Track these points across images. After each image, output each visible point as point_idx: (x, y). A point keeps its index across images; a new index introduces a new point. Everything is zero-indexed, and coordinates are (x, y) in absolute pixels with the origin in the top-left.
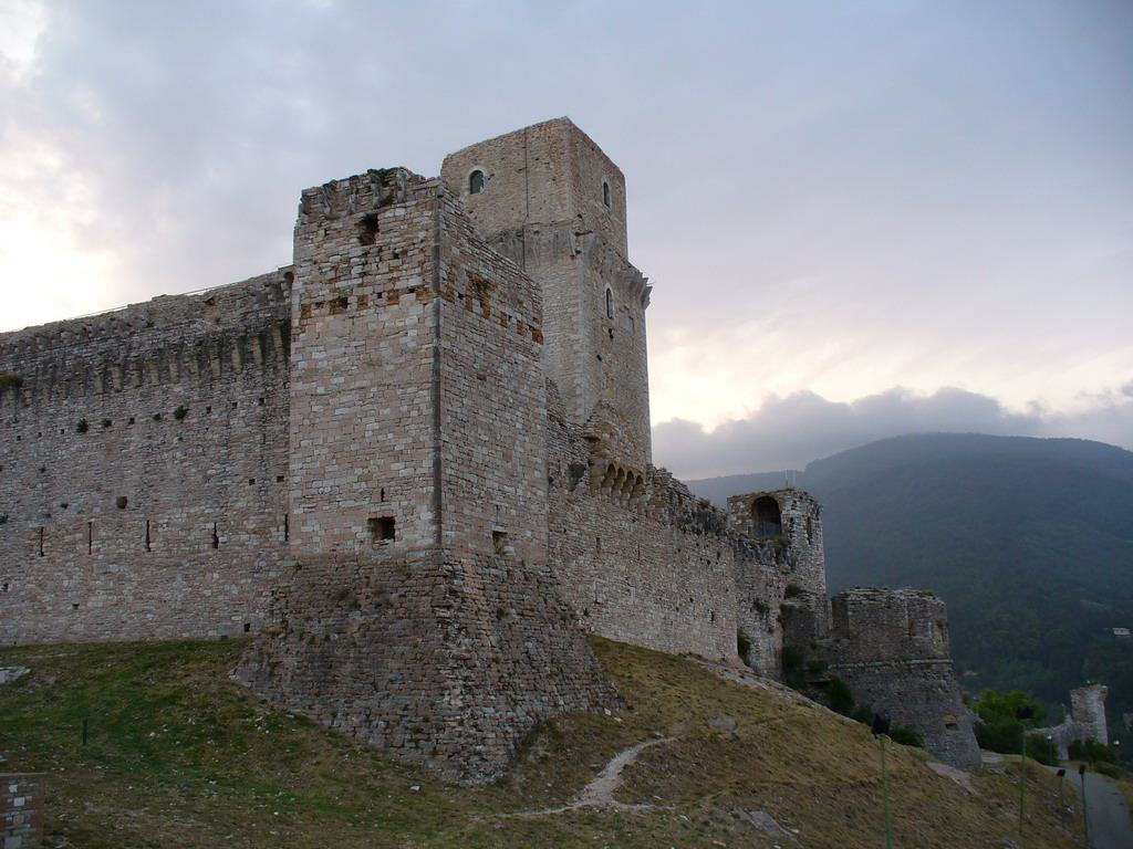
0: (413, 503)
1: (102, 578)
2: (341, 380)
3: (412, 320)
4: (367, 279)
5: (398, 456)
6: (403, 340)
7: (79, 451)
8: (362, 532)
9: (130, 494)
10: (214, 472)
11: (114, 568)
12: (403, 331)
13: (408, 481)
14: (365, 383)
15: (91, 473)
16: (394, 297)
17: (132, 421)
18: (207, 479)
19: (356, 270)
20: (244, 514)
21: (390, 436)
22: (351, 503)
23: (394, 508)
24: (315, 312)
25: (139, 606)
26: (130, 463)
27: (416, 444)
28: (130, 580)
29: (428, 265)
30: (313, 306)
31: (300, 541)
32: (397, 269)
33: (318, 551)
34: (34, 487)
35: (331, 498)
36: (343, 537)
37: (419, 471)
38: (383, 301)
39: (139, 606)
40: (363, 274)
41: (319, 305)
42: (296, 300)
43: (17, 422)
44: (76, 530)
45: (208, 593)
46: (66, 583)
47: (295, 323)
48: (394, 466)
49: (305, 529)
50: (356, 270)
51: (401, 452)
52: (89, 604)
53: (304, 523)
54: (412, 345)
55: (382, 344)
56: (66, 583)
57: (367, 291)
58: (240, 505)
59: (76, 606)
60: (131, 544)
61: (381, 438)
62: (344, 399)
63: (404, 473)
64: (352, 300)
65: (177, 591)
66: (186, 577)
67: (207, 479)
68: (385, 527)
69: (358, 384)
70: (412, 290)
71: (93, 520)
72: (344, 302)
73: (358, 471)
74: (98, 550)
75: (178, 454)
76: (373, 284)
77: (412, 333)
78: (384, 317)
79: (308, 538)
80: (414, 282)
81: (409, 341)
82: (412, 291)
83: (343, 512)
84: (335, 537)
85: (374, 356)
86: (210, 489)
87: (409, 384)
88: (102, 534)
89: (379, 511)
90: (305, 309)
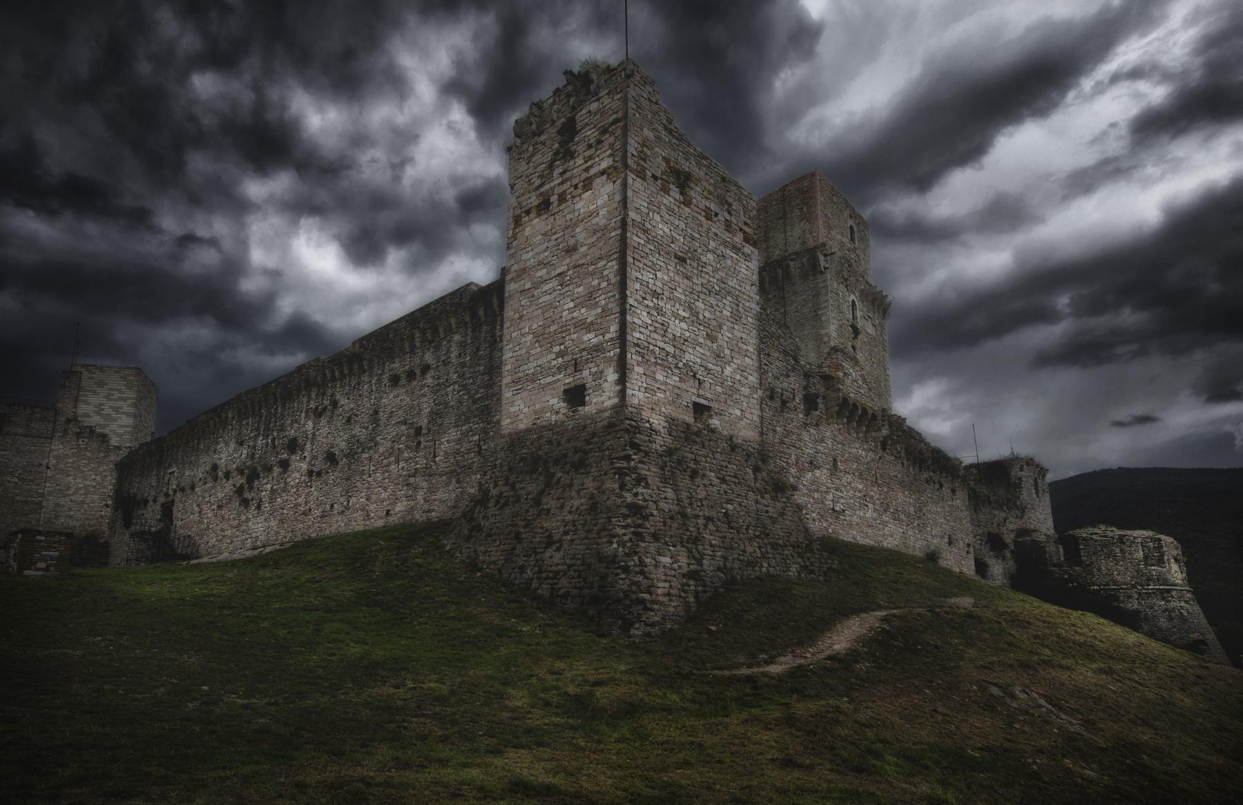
0: (601, 367)
6: (594, 221)
8: (556, 402)
9: (424, 422)
10: (480, 395)
11: (412, 480)
13: (598, 349)
15: (401, 412)
18: (475, 402)
21: (583, 310)
22: (549, 379)
29: (618, 145)
30: (523, 215)
31: (509, 421)
32: (590, 158)
36: (543, 410)
37: (608, 336)
48: (586, 338)
49: (512, 410)
51: (592, 323)
55: (578, 230)
61: (575, 314)
62: (546, 288)
63: (595, 341)
64: (554, 199)
66: (458, 481)
67: (475, 402)
68: (576, 396)
69: (558, 271)
73: (556, 349)
77: (603, 212)
83: (543, 387)
84: (536, 412)
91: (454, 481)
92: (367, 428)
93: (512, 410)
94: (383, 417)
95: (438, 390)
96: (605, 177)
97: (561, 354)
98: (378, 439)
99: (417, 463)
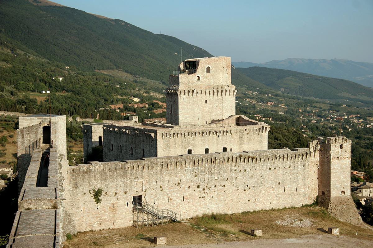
1: (276, 197)
2: (338, 170)
4: (342, 155)
5: (346, 182)
6: (346, 165)
11: (278, 196)
14: (341, 171)
18: (294, 179)
19: (340, 153)
20: (301, 186)
22: (339, 189)
23: (345, 190)
24: (334, 159)
25: (283, 202)
26: (280, 176)
28: (281, 198)
33: (335, 196)
35: (336, 188)
36: (338, 194)
38: (344, 158)
39: (283, 202)
40: (341, 154)
41: (335, 158)
42: (331, 157)
43: (254, 166)
44: (270, 189)
45: (296, 199)
46: (268, 199)
47: (331, 160)
48: (345, 184)
49: (333, 193)
50: (340, 153)
52: (274, 202)
53: (333, 192)
56: (268, 199)
57: (342, 157)
58: (301, 184)
65: (290, 200)
66: (292, 197)
67: (294, 179)
71: (273, 187)
72: (338, 158)
76: (343, 156)
79: (333, 194)
80: (348, 156)
83: (338, 190)
85: (342, 167)
86: (295, 181)
88: (275, 189)
89: (343, 190)
91: (291, 197)
93: (333, 193)
95: (283, 174)
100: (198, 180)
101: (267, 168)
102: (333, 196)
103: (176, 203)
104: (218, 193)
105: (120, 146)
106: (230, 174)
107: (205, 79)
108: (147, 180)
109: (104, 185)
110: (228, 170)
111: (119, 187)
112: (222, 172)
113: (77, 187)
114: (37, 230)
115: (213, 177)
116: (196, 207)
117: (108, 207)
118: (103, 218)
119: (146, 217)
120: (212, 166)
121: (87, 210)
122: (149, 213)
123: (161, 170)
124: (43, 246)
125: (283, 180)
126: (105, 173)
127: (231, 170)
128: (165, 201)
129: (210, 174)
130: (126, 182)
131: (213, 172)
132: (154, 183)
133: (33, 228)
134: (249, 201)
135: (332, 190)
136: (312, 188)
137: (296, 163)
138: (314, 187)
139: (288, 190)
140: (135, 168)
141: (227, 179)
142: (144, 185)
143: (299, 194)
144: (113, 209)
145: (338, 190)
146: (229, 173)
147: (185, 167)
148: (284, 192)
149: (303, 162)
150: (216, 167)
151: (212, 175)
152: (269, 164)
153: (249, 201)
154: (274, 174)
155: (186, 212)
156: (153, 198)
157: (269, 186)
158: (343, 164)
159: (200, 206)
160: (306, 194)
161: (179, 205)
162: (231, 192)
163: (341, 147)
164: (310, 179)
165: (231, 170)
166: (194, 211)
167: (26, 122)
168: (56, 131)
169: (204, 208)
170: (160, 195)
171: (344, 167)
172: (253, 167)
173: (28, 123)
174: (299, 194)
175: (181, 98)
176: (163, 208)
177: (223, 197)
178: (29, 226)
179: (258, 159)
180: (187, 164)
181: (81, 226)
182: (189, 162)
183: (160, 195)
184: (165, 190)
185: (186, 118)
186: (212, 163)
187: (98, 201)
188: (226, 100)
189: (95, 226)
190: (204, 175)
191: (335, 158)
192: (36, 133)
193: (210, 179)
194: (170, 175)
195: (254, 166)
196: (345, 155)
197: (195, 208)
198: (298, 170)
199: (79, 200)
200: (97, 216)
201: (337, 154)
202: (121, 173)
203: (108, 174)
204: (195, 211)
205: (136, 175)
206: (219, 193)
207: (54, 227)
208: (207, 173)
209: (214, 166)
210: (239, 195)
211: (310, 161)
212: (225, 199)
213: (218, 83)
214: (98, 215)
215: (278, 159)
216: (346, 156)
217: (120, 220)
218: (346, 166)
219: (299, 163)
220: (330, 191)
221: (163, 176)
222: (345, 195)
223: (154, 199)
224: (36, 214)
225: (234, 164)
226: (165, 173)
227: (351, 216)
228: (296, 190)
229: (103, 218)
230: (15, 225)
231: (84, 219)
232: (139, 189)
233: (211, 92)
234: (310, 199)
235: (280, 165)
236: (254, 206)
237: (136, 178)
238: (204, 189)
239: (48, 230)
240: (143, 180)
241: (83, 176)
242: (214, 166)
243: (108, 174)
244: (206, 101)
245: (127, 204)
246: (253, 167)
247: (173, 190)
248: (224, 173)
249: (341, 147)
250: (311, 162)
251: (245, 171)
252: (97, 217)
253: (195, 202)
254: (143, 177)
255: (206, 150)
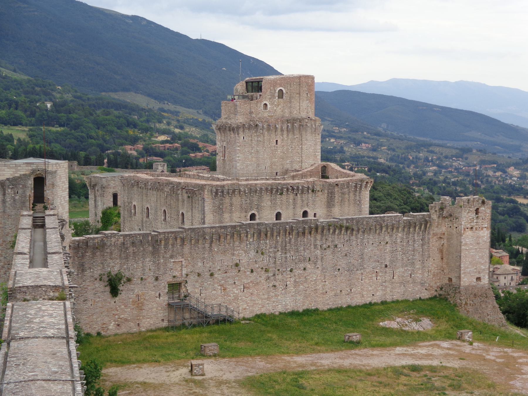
2: (472, 246)
3: (485, 234)
4: (478, 224)
5: (482, 264)
7: (371, 250)
8: (475, 280)
9: (388, 264)
12: (484, 237)
13: (484, 270)
16: (482, 229)
17: (387, 243)
19: (475, 221)
22: (473, 274)
23: (481, 275)
24: (467, 230)
26: (387, 255)
27: (486, 262)
33: (466, 285)
34: (358, 261)
35: (469, 273)
38: (480, 229)
39: (391, 294)
41: (467, 228)
43: (350, 240)
44: (373, 273)
45: (410, 290)
46: (370, 288)
47: (462, 232)
49: (464, 280)
50: (475, 221)
52: (377, 294)
54: (485, 240)
56: (370, 288)
57: (477, 226)
58: (417, 267)
59: (373, 295)
60: (388, 277)
64: (474, 228)
66: (404, 286)
68: (478, 279)
70: (485, 227)
73: (475, 267)
74: (379, 279)
75: (401, 253)
77: (486, 237)
78: (480, 233)
80: (486, 226)
81: (485, 239)
82: (485, 227)
83: (472, 276)
84: (470, 281)
85: (478, 242)
86: (409, 262)
87: (485, 249)
89: (478, 276)
90: (464, 229)
91: (402, 286)
92: (358, 261)
93: (464, 280)
94: (366, 258)
95: (392, 252)
96: (486, 229)
97: (476, 269)
98: (365, 266)
99: (385, 278)
100: (265, 261)
101: (368, 242)
102: (464, 284)
103: (232, 295)
104: (295, 281)
105: (148, 208)
106: (314, 252)
107: (275, 108)
108: (189, 259)
109: (125, 267)
110: (311, 245)
111: (147, 270)
112: (302, 248)
113: (83, 271)
114: (41, 331)
115: (288, 256)
116: (262, 299)
117: (131, 300)
118: (122, 316)
119: (187, 316)
120: (287, 240)
121: (100, 304)
122: (192, 309)
123: (211, 246)
124: (54, 354)
125: (392, 262)
126: (127, 248)
127: (315, 246)
128: (214, 292)
129: (284, 251)
130: (158, 262)
131: (288, 248)
132: (200, 264)
133: (35, 328)
134: (341, 291)
135: (462, 276)
136: (434, 273)
137: (411, 235)
138: (436, 271)
139: (398, 276)
140: (171, 242)
141: (309, 260)
142: (185, 267)
143: (414, 282)
144: (139, 304)
145: (472, 276)
146: (313, 249)
147: (247, 241)
148: (393, 278)
149: (421, 234)
150: (293, 240)
151: (286, 253)
152: (371, 238)
153: (341, 291)
154: (378, 253)
155: (247, 307)
156: (198, 287)
157: (371, 269)
158: (480, 238)
159: (268, 299)
160: (425, 282)
161: (236, 298)
162: (314, 278)
163: (477, 211)
164: (431, 259)
165: (315, 246)
166: (259, 306)
167: (8, 170)
168: (53, 185)
169: (274, 302)
170: (209, 283)
171: (481, 241)
172: (347, 241)
173: (12, 173)
174: (414, 282)
175: (239, 137)
176: (213, 302)
177: (302, 286)
178: (28, 325)
179: (355, 228)
180: (249, 236)
181: (90, 328)
182: (252, 232)
183: (209, 283)
184: (216, 276)
185: (247, 166)
186: (287, 235)
187: (114, 292)
188: (307, 140)
189: (110, 327)
190: (275, 253)
191: (467, 228)
192: (24, 186)
193: (284, 259)
194: (224, 252)
195: (350, 240)
196: (482, 225)
197: (260, 302)
198: (414, 246)
199: (86, 290)
200: (113, 312)
201: (471, 223)
202: (151, 248)
203: (131, 250)
204: (261, 306)
205: (173, 251)
206: (297, 280)
207: (64, 327)
208: (280, 249)
209: (290, 240)
210: (327, 283)
211: (431, 232)
212: (305, 289)
213: (295, 114)
214: (115, 312)
215: (384, 229)
216: (484, 226)
217: (148, 320)
218: (484, 241)
219: (416, 235)
220: (459, 277)
221: (213, 254)
222: (481, 283)
223: (200, 289)
224: (36, 307)
225: (319, 237)
226: (216, 250)
227: (489, 314)
228: (411, 275)
229: (122, 316)
230: (7, 323)
231: (95, 317)
232: (177, 274)
233: (285, 127)
234: (431, 289)
235: (387, 238)
236: (349, 299)
237: (172, 257)
238: (274, 275)
239: (56, 331)
240: (183, 260)
241: (94, 254)
242: (290, 240)
243: (131, 250)
244: (277, 141)
245: (160, 295)
246: (347, 241)
247: (228, 274)
248: (304, 250)
249: (477, 211)
250: (433, 234)
251: (336, 246)
252: (113, 314)
253: (261, 293)
254: (183, 255)
255: (277, 215)
